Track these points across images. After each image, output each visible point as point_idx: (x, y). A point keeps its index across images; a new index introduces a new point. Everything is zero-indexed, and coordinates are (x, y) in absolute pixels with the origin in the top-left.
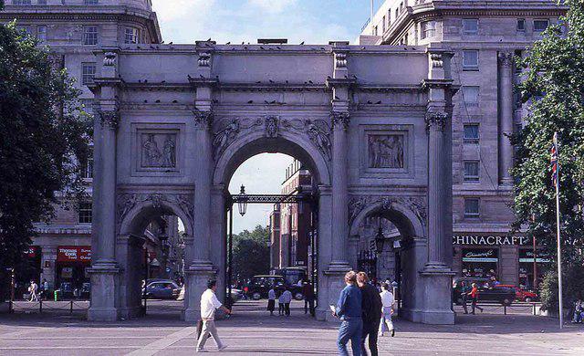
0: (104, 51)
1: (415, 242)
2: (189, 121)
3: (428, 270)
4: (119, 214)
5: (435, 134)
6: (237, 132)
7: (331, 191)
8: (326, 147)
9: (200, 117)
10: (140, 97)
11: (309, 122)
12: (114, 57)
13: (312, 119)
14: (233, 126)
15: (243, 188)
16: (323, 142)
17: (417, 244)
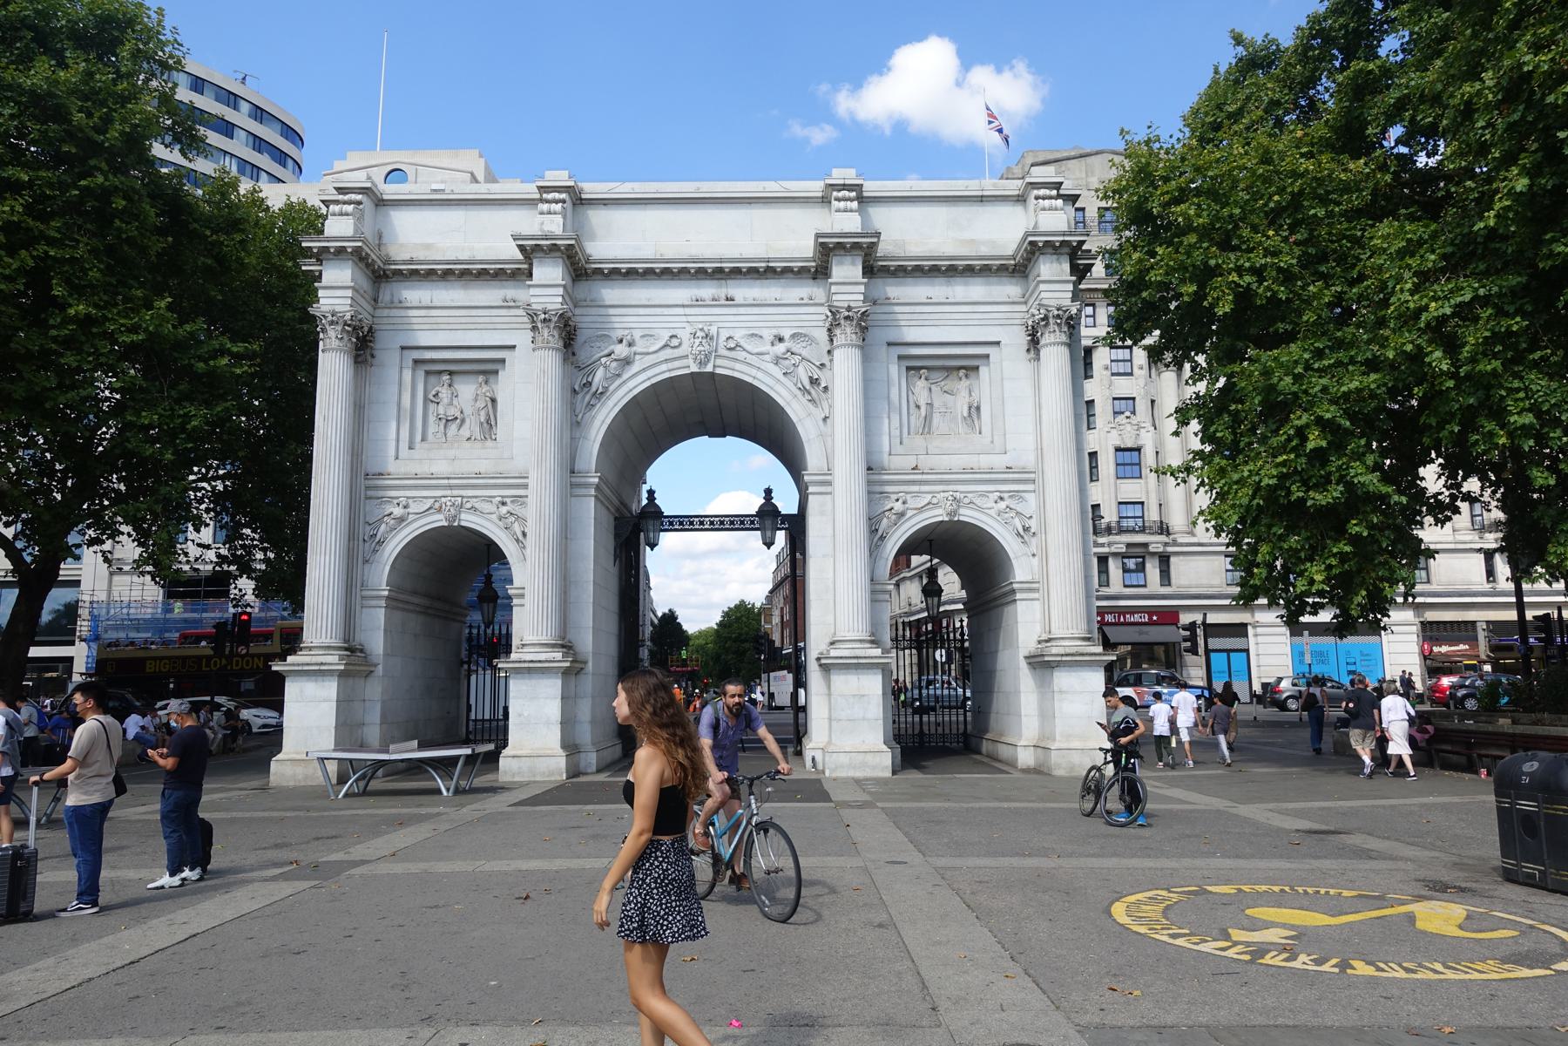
0: (340, 190)
1: (1013, 591)
2: (522, 338)
3: (1054, 651)
4: (360, 541)
5: (1055, 356)
6: (627, 362)
7: (829, 483)
8: (815, 387)
9: (536, 321)
10: (414, 294)
11: (781, 340)
12: (359, 203)
13: (786, 334)
14: (621, 350)
15: (651, 493)
16: (814, 382)
17: (1018, 596)
